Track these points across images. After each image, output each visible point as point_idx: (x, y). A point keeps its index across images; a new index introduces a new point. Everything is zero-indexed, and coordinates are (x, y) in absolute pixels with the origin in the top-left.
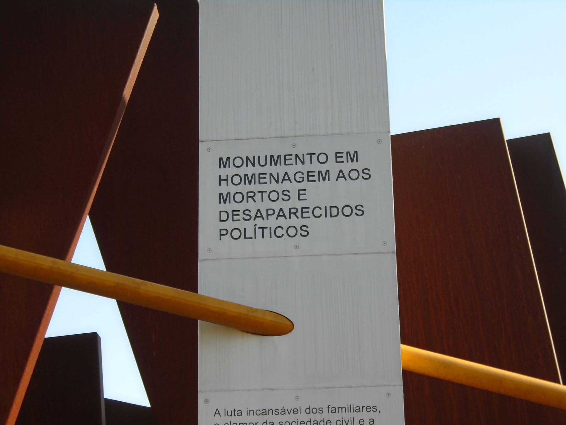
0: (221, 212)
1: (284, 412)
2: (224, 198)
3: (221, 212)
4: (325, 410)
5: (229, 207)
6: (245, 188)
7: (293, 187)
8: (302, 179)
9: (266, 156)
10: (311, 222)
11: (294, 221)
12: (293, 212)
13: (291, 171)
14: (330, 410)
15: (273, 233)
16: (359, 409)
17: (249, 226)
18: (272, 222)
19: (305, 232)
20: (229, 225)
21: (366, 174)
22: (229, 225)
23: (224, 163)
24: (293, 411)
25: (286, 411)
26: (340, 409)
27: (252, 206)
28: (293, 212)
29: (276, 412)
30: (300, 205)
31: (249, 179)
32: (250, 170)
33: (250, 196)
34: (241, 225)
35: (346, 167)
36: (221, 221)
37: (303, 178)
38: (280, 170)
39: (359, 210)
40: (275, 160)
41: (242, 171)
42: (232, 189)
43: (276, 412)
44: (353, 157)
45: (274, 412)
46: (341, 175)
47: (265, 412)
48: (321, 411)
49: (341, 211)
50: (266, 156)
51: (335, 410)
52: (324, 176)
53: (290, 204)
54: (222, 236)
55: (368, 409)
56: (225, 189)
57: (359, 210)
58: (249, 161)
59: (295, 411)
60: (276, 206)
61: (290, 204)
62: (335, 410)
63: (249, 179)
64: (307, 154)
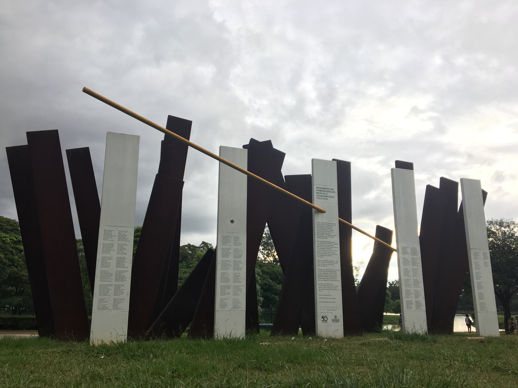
2: (317, 193)
5: (318, 194)
6: (320, 192)
7: (326, 193)
10: (328, 198)
11: (326, 197)
13: (325, 190)
15: (323, 199)
16: (334, 224)
17: (320, 197)
18: (323, 197)
19: (327, 199)
20: (318, 197)
21: (334, 192)
22: (318, 197)
23: (317, 188)
27: (321, 195)
30: (327, 195)
31: (320, 191)
32: (320, 189)
33: (320, 193)
34: (319, 197)
35: (332, 191)
38: (324, 190)
39: (334, 197)
40: (323, 188)
41: (319, 189)
42: (318, 192)
43: (324, 223)
44: (333, 190)
47: (323, 223)
49: (331, 197)
51: (331, 224)
52: (329, 192)
53: (325, 195)
55: (335, 224)
57: (334, 197)
59: (326, 223)
60: (324, 195)
61: (325, 195)
62: (331, 224)
63: (320, 191)
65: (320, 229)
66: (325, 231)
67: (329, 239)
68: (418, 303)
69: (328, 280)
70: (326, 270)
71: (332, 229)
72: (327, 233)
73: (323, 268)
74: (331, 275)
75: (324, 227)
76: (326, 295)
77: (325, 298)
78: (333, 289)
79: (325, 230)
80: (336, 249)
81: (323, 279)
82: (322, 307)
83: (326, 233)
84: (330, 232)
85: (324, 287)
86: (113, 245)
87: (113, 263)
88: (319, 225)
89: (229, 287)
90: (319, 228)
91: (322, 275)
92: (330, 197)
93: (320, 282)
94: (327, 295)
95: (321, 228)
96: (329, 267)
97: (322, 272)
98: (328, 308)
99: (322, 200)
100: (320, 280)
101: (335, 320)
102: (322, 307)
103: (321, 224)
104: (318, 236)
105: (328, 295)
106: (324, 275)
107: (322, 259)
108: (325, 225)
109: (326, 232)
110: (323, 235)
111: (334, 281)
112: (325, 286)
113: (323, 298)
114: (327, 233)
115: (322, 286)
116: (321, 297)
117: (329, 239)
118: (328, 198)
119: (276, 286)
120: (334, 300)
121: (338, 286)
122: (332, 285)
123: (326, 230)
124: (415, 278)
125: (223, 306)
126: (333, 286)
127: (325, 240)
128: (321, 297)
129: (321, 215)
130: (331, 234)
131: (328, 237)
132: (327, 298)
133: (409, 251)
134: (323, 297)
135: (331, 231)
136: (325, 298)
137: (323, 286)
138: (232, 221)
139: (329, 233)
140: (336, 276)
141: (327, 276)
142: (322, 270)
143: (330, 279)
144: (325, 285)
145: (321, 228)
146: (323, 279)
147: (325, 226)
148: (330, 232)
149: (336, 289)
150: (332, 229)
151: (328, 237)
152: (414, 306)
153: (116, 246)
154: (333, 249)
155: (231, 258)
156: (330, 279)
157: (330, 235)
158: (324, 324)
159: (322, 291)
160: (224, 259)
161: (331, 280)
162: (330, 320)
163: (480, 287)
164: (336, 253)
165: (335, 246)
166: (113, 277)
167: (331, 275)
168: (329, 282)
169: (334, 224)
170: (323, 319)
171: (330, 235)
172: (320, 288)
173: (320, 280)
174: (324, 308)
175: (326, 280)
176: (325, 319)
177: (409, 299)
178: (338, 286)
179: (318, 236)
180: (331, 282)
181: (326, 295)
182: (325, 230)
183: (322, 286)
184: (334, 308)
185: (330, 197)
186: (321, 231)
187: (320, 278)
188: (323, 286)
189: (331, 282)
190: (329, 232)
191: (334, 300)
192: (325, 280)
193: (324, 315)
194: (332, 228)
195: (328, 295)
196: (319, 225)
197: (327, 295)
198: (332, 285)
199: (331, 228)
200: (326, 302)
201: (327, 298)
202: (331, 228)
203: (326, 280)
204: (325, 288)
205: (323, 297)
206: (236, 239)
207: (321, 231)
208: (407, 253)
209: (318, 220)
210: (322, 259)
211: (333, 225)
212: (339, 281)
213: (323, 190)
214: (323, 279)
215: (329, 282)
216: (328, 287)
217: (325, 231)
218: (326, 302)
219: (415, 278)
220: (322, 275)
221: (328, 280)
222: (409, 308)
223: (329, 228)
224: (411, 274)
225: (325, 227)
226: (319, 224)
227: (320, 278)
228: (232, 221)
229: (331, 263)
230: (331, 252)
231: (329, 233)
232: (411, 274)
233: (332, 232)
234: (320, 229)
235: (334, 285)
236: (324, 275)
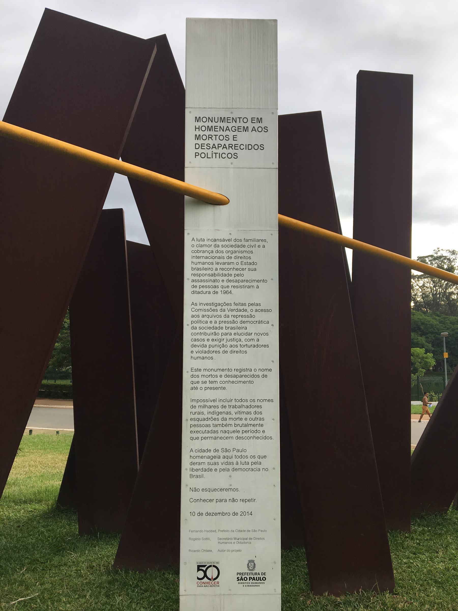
0: (196, 144)
1: (224, 240)
2: (197, 137)
3: (196, 144)
4: (243, 240)
5: (200, 142)
6: (207, 133)
8: (235, 130)
9: (218, 117)
10: (238, 152)
11: (231, 151)
12: (230, 146)
13: (230, 125)
14: (245, 240)
15: (221, 156)
16: (258, 241)
17: (209, 152)
18: (220, 151)
19: (235, 156)
20: (200, 151)
21: (266, 129)
22: (200, 151)
23: (198, 119)
24: (228, 240)
25: (225, 240)
26: (250, 240)
27: (211, 142)
28: (230, 146)
29: (220, 240)
30: (234, 143)
31: (209, 129)
32: (210, 124)
33: (210, 137)
34: (205, 151)
35: (256, 125)
36: (196, 148)
37: (236, 129)
38: (224, 125)
39: (262, 147)
40: (222, 120)
41: (206, 124)
42: (201, 133)
43: (220, 240)
44: (260, 120)
45: (219, 240)
46: (254, 129)
47: (215, 240)
48: (241, 240)
49: (253, 147)
50: (218, 117)
51: (247, 241)
52: (246, 129)
53: (229, 142)
54: (196, 129)
55: (262, 240)
56: (198, 133)
57: (262, 147)
58: (210, 119)
59: (229, 240)
60: (222, 143)
61: (229, 142)
62: (247, 241)
63: (209, 129)
64: (238, 118)
65: (204, 263)
66: (223, 269)
69: (227, 435)
70: (220, 400)
71: (250, 258)
72: (231, 275)
73: (209, 395)
74: (241, 419)
75: (218, 255)
76: (215, 490)
77: (211, 501)
78: (245, 466)
79: (224, 264)
80: (263, 328)
81: (209, 432)
82: (201, 531)
83: (225, 275)
84: (243, 269)
85: (209, 460)
88: (200, 249)
90: (198, 257)
91: (204, 419)
92: (249, 147)
93: (197, 445)
94: (221, 490)
95: (207, 258)
97: (205, 410)
98: (221, 535)
99: (216, 162)
100: (197, 438)
102: (201, 531)
103: (210, 243)
104: (196, 287)
105: (227, 490)
106: (215, 419)
107: (209, 364)
108: (223, 246)
109: (226, 272)
110: (214, 281)
111: (251, 440)
112: (215, 457)
113: (204, 501)
114: (231, 275)
115: (202, 457)
116: (196, 495)
119: (418, 339)
120: (247, 507)
121: (265, 457)
122: (243, 454)
123: (229, 264)
126: (247, 457)
127: (221, 298)
128: (196, 495)
130: (248, 275)
131: (234, 287)
132: (221, 501)
134: (206, 495)
135: (244, 267)
136: (211, 501)
137: (209, 457)
139: (239, 272)
140: (261, 422)
141: (224, 423)
142: (205, 403)
143: (234, 432)
144: (216, 454)
145: (207, 258)
146: (209, 435)
147: (222, 252)
148: (243, 269)
149: (258, 466)
150: (250, 258)
151: (234, 287)
154: (251, 328)
156: (234, 432)
157: (243, 281)
158: (203, 590)
159: (202, 476)
161: (240, 435)
164: (264, 340)
165: (259, 316)
167: (241, 419)
168: (234, 444)
169: (258, 241)
170: (201, 574)
171: (243, 281)
172: (195, 467)
173: (197, 438)
174: (204, 535)
175: (221, 438)
176: (211, 573)
178: (265, 457)
179: (196, 287)
180: (239, 444)
181: (215, 490)
182: (224, 264)
183: (202, 457)
184: (251, 535)
185: (249, 147)
186: (206, 269)
187: (197, 432)
188: (209, 457)
189: (239, 444)
190: (237, 269)
191: (247, 507)
192: (216, 438)
193: (205, 559)
194: (250, 255)
195: (227, 490)
196: (200, 249)
197: (221, 490)
198: (243, 454)
199: (248, 255)
200: (216, 514)
201: (221, 501)
202: (248, 255)
203: (221, 438)
204: (215, 464)
205: (206, 495)
207: (206, 269)
210: (209, 364)
211: (257, 244)
212: (271, 438)
213: (220, 124)
214: (209, 435)
215: (234, 444)
216: (226, 460)
217: (223, 269)
218: (216, 514)
220: (204, 419)
221: (227, 435)
223: (241, 255)
225: (223, 255)
226: (202, 246)
227: (197, 432)
230: (243, 338)
231: (239, 272)
233: (249, 270)
234: (204, 263)
235: (248, 453)
236: (215, 419)
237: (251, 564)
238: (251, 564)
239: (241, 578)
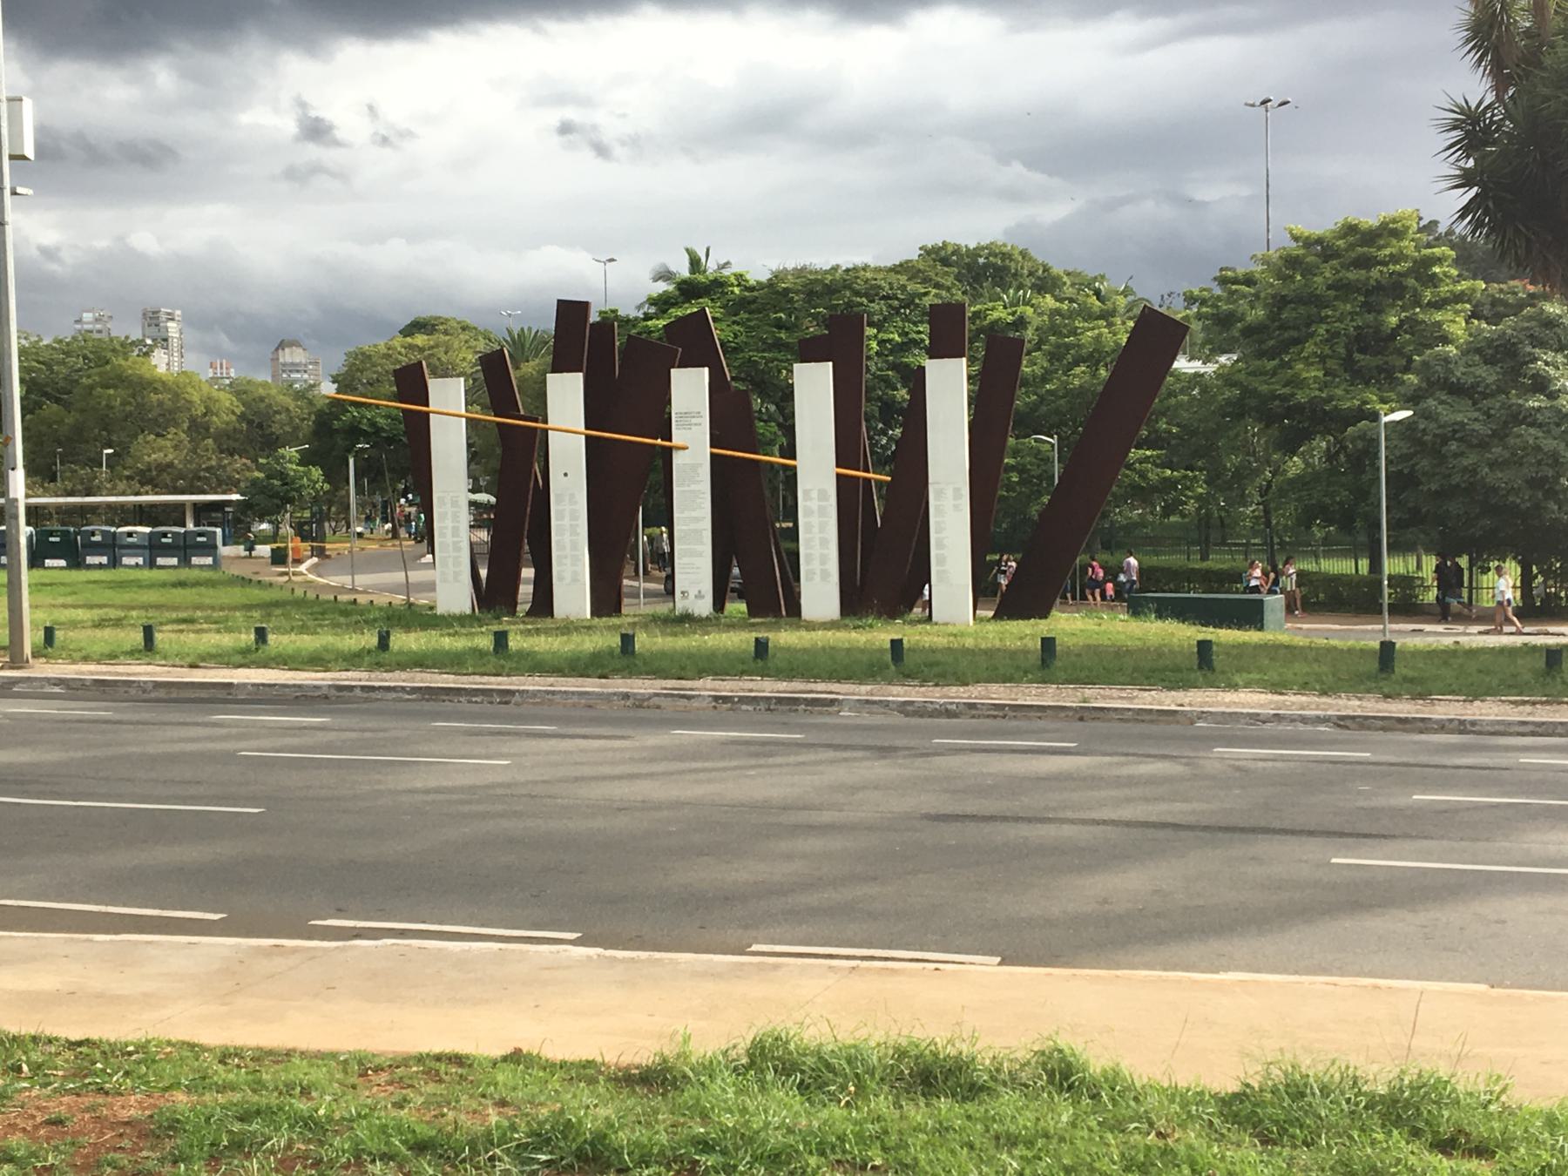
67: (693, 487)
68: (825, 575)
73: (684, 528)
86: (447, 513)
87: (449, 532)
89: (566, 557)
92: (696, 424)
96: (692, 526)
101: (699, 596)
117: (693, 487)
118: (693, 427)
124: (821, 535)
125: (561, 579)
127: (687, 488)
129: (681, 453)
133: (814, 494)
138: (566, 475)
152: (817, 578)
153: (450, 514)
155: (567, 522)
160: (559, 523)
162: (692, 596)
163: (940, 545)
165: (702, 496)
166: (451, 548)
177: (810, 567)
185: (696, 424)
193: (683, 589)
206: (572, 496)
208: (811, 499)
209: (678, 459)
210: (683, 515)
215: (692, 547)
219: (821, 535)
222: (809, 579)
224: (816, 530)
228: (566, 475)
229: (697, 520)
232: (816, 530)
237: (700, 592)
238: (700, 592)
239: (696, 596)
